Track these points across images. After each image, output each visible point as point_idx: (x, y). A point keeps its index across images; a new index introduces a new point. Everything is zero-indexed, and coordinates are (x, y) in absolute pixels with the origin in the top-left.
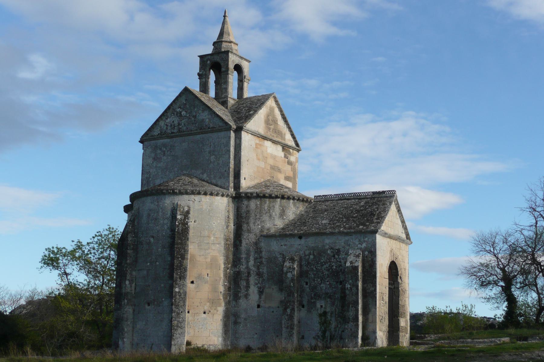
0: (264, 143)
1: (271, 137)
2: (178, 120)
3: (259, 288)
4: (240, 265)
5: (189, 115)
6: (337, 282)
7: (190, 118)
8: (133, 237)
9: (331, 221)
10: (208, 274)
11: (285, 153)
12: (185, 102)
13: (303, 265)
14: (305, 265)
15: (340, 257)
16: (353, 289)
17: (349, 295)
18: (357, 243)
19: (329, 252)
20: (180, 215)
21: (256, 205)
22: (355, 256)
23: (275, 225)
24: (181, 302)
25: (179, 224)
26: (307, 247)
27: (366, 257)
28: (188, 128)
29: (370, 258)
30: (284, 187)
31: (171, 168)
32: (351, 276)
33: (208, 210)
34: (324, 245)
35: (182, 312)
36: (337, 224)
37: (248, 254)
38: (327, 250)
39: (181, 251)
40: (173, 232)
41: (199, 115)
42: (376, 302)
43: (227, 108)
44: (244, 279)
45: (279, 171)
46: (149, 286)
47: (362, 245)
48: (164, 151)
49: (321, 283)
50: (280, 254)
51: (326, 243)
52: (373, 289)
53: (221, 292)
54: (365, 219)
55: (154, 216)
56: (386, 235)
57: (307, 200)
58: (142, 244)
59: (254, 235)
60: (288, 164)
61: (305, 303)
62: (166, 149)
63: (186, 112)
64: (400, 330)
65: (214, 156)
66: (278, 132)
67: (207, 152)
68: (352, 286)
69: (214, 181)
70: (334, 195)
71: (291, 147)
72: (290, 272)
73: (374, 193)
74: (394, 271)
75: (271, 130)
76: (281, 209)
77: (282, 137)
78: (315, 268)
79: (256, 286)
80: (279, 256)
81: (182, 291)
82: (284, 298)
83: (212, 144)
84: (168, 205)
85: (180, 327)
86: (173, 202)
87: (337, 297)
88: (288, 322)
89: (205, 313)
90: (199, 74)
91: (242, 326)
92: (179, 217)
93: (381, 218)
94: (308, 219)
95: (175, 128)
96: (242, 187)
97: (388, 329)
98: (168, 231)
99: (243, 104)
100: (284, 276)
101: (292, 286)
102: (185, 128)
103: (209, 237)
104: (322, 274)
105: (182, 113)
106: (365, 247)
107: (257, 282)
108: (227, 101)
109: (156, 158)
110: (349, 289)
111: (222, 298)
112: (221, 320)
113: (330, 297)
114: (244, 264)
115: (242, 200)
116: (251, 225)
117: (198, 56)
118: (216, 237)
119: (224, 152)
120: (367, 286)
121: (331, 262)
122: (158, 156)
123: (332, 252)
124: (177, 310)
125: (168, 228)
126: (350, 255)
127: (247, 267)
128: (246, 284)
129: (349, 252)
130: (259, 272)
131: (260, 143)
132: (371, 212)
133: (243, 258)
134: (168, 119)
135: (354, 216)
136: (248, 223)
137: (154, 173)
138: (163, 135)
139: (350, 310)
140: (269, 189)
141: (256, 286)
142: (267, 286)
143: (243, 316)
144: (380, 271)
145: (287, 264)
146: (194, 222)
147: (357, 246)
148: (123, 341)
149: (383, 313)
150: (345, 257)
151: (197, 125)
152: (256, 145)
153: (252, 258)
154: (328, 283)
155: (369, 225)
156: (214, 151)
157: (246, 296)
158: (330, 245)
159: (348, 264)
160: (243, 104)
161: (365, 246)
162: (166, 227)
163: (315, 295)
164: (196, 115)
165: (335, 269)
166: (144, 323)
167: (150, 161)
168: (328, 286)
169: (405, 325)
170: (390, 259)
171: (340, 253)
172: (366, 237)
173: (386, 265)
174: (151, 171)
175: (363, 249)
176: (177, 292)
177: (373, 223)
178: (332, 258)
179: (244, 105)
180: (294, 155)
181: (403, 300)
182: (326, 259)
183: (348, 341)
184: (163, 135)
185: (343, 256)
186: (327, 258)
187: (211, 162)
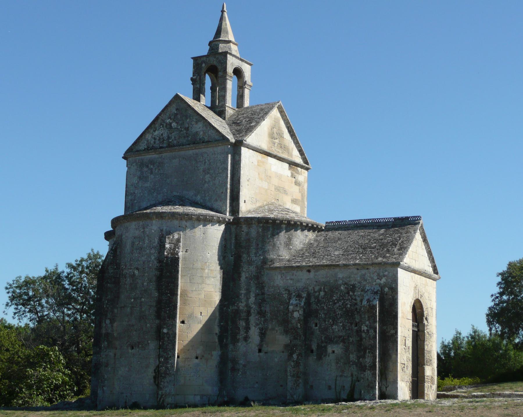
0: (267, 159)
1: (275, 153)
2: (167, 133)
3: (261, 329)
4: (239, 303)
5: (181, 127)
6: (351, 324)
7: (181, 131)
8: (115, 269)
9: (345, 251)
10: (201, 313)
11: (293, 172)
12: (176, 112)
13: (312, 303)
14: (314, 303)
15: (355, 294)
16: (370, 331)
17: (365, 339)
18: (375, 278)
19: (342, 288)
20: (169, 243)
21: (258, 232)
22: (372, 293)
23: (280, 256)
24: (170, 345)
25: (168, 254)
26: (317, 282)
27: (386, 294)
28: (179, 142)
29: (390, 295)
30: (291, 211)
31: (159, 189)
32: (368, 317)
33: (201, 238)
34: (337, 280)
35: (170, 357)
36: (352, 255)
37: (248, 291)
38: (341, 285)
39: (171, 285)
40: (161, 264)
41: (191, 127)
42: (397, 347)
43: (224, 119)
44: (244, 319)
45: (285, 192)
46: (133, 326)
47: (381, 280)
48: (152, 169)
49: (333, 324)
50: (286, 290)
51: (339, 278)
52: (393, 332)
53: (216, 334)
54: (386, 249)
55: (139, 245)
56: (408, 269)
57: (317, 226)
58: (125, 277)
59: (255, 268)
60: (296, 184)
61: (314, 347)
62: (154, 166)
63: (177, 123)
64: (426, 380)
65: (209, 175)
66: (285, 147)
67: (201, 170)
68: (369, 329)
69: (209, 204)
70: (349, 221)
71: (299, 164)
72: (296, 311)
73: (395, 219)
74: (420, 310)
75: (276, 145)
76: (287, 236)
77: (288, 153)
78: (326, 306)
79: (258, 327)
80: (284, 293)
81: (171, 332)
82: (289, 341)
83: (206, 160)
84: (155, 231)
85: (168, 374)
86: (161, 228)
87: (351, 341)
88: (294, 369)
89: (197, 358)
90: (192, 79)
91: (240, 373)
92: (167, 246)
93: (403, 249)
94: (319, 250)
95: (165, 142)
96: (241, 212)
97: (411, 379)
98: (155, 262)
99: (243, 114)
100: (290, 315)
101: (299, 327)
102: (175, 142)
103: (203, 269)
104: (334, 313)
105: (172, 125)
106: (384, 282)
107: (258, 322)
108: (225, 110)
109: (142, 177)
110: (365, 331)
111: (217, 340)
112: (216, 366)
113: (343, 341)
114: (243, 301)
115: (242, 227)
116: (252, 256)
117: (192, 58)
118: (211, 270)
119: (221, 170)
120: (387, 328)
121: (345, 300)
122: (144, 175)
123: (345, 288)
124: (165, 354)
125: (155, 259)
126: (367, 292)
127: (247, 305)
128: (245, 325)
129: (366, 289)
130: (261, 310)
132: (392, 241)
133: (242, 294)
134: (156, 131)
135: (372, 246)
136: (248, 253)
137: (139, 195)
138: (149, 149)
139: (367, 356)
140: (272, 213)
141: (258, 327)
142: (270, 327)
143: (242, 362)
144: (402, 310)
145: (293, 301)
146: (186, 252)
147: (376, 282)
148: (103, 390)
149: (406, 361)
150: (361, 294)
151: (189, 139)
152: (258, 162)
153: (252, 295)
154: (341, 324)
155: (390, 256)
156: (209, 169)
157: (246, 339)
158: (344, 280)
159: (365, 303)
160: (243, 114)
161: (385, 281)
162: (153, 258)
163: (325, 338)
164: (188, 127)
165: (349, 308)
166: (127, 369)
167: (135, 180)
168: (342, 328)
169: (431, 374)
170: (414, 296)
171: (356, 289)
172: (386, 271)
173: (409, 304)
174: (136, 192)
175: (382, 285)
176: (165, 333)
177: (395, 254)
178: (346, 295)
179: (245, 115)
180: (303, 174)
181: (430, 345)
182: (339, 296)
183: (364, 392)
184: (149, 149)
185: (359, 293)
186: (340, 295)
187: (205, 182)
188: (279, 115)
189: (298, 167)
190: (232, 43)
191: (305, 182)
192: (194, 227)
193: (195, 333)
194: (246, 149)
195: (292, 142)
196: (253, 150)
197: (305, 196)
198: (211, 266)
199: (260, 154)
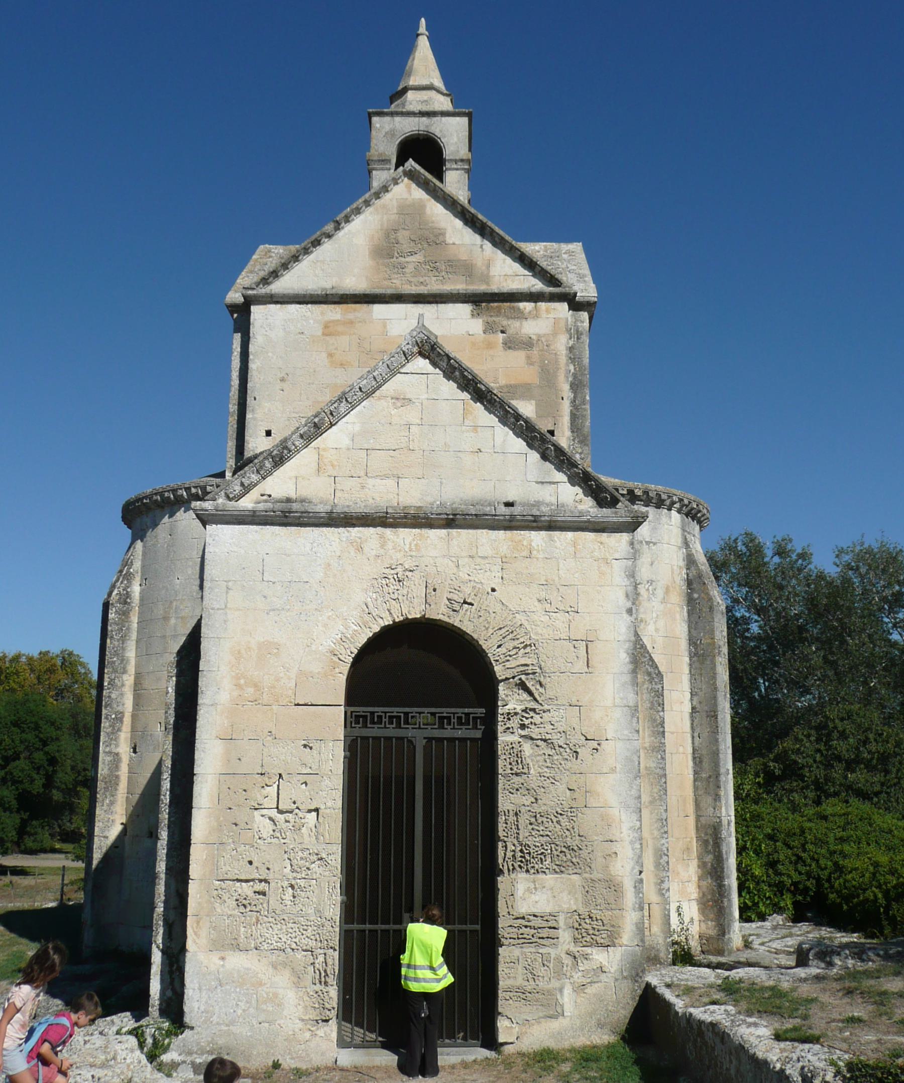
11: (490, 319)
33: (166, 546)
103: (166, 618)
118: (182, 618)
131: (351, 316)
180: (544, 315)
188: (419, 194)
190: (412, 89)
191: (555, 334)
192: (155, 525)
193: (149, 775)
194: (272, 306)
195: (488, 245)
196: (300, 303)
197: (558, 369)
198: (182, 607)
199: (336, 306)
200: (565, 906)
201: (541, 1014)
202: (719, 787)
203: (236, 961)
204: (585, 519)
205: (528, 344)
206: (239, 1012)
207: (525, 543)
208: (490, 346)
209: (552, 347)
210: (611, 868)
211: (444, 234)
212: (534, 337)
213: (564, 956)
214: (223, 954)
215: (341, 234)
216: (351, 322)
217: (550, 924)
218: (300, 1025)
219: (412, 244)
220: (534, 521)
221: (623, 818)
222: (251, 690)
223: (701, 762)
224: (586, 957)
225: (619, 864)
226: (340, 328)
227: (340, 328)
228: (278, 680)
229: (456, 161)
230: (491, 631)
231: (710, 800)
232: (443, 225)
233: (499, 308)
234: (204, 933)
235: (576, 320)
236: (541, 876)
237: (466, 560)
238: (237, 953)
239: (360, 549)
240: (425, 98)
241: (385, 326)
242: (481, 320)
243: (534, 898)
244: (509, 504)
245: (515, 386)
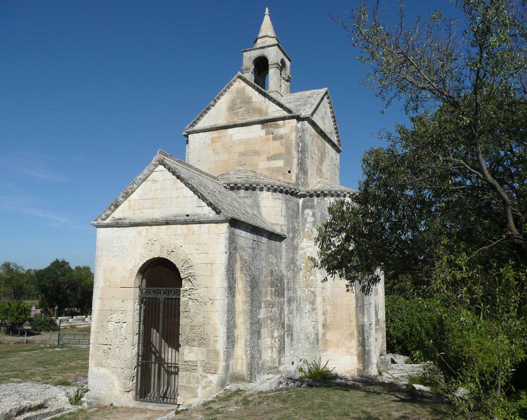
45: (257, 153)
131: (220, 135)
152: (212, 140)
189: (278, 121)
191: (291, 132)
196: (204, 132)
197: (292, 146)
200: (200, 359)
201: (191, 396)
202: (364, 310)
203: (102, 370)
204: (209, 219)
205: (281, 138)
206: (102, 387)
207: (192, 229)
208: (268, 140)
209: (290, 138)
210: (216, 346)
211: (252, 99)
212: (283, 135)
213: (199, 376)
214: (98, 368)
215: (217, 104)
216: (220, 137)
217: (195, 365)
218: (119, 392)
219: (241, 104)
220: (194, 221)
221: (221, 328)
222: (108, 283)
223: (358, 299)
224: (206, 377)
225: (218, 345)
226: (217, 140)
227: (217, 140)
228: (115, 279)
229: (273, 65)
230: (180, 261)
231: (361, 315)
232: (251, 95)
233: (271, 124)
234: (93, 361)
235: (302, 125)
236: (192, 348)
237: (173, 236)
238: (103, 368)
239: (140, 234)
240: (264, 41)
241: (232, 137)
242: (264, 130)
243: (190, 355)
244: (188, 216)
245: (277, 155)
